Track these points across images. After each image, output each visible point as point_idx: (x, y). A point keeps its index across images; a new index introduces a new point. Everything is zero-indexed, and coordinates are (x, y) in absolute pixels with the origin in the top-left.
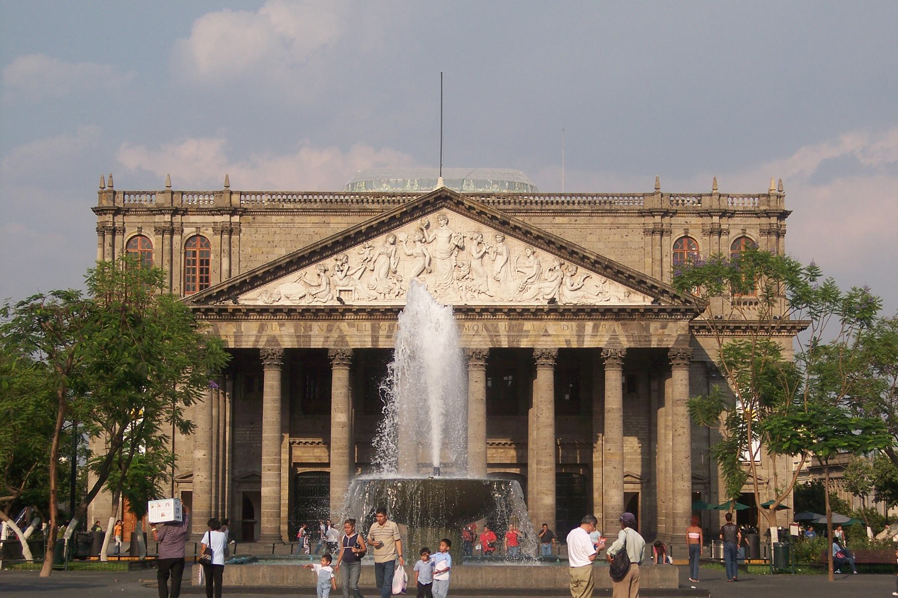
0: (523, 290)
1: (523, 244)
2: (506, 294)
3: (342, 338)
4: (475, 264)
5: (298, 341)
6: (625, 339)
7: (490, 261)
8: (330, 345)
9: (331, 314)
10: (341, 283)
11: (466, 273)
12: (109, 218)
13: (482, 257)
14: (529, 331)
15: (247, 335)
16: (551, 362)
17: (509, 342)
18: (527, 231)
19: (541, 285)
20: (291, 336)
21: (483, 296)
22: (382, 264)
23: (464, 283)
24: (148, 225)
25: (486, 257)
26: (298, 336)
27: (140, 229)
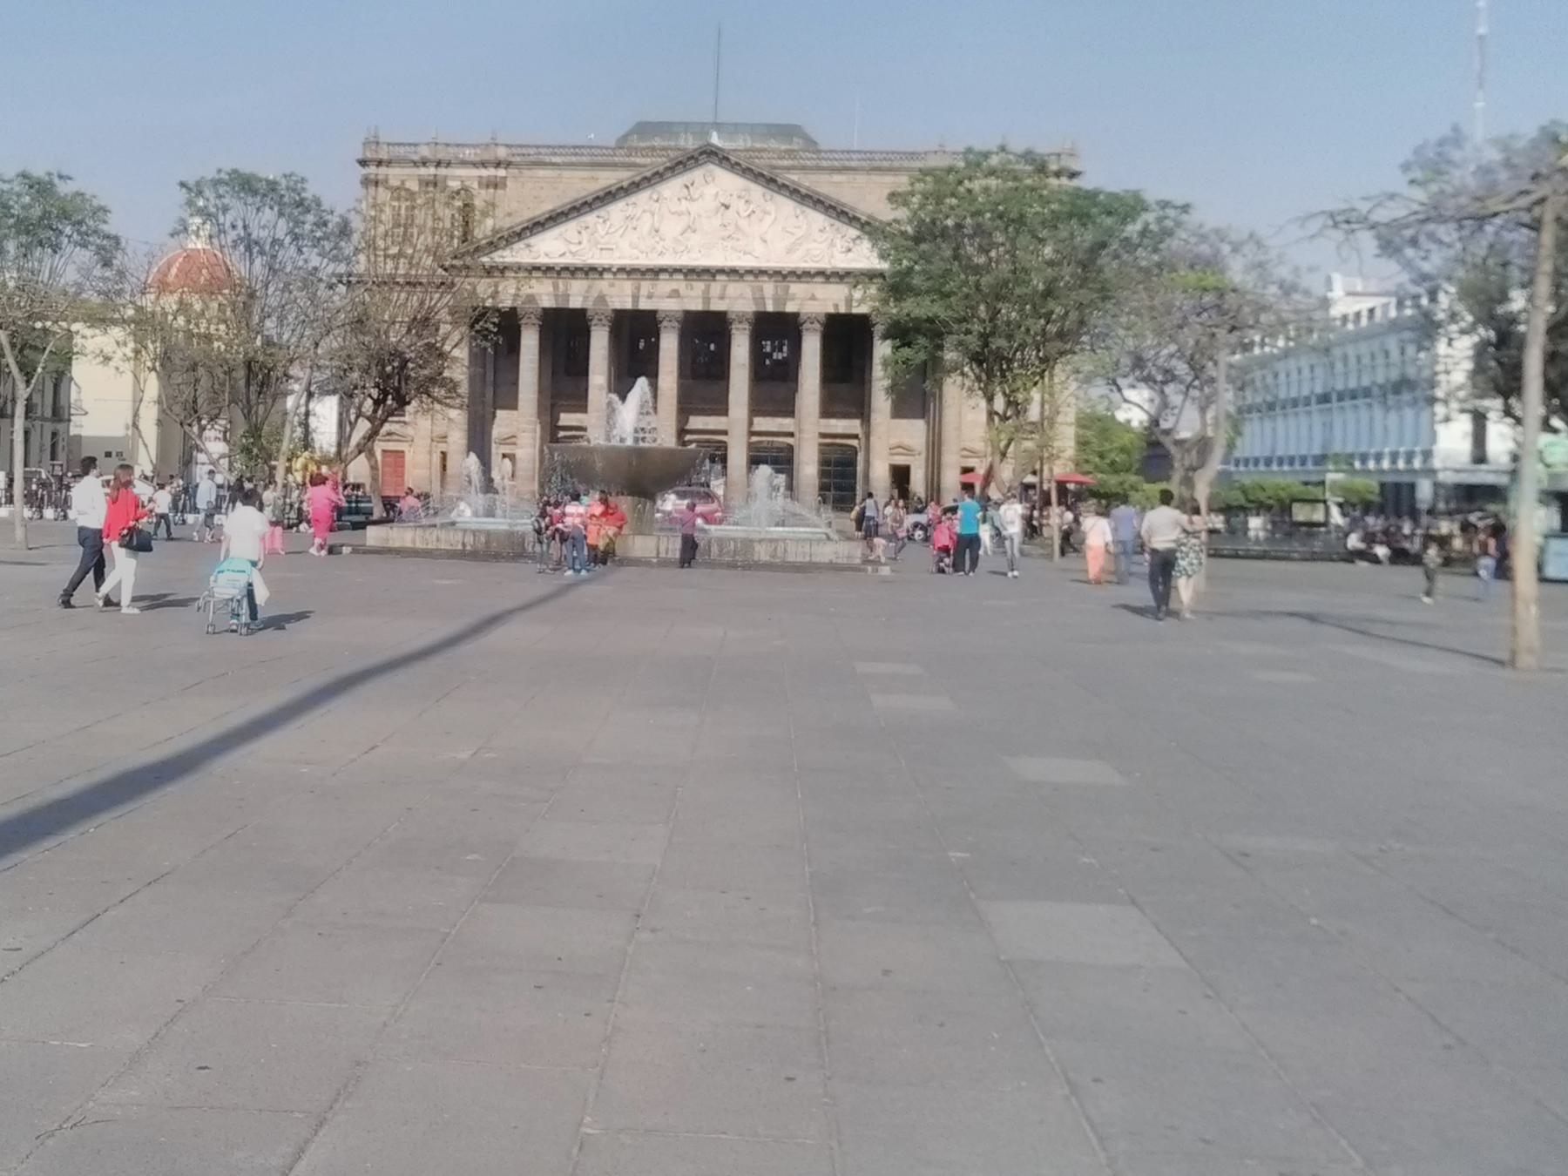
0: (789, 251)
3: (601, 298)
4: (743, 223)
8: (589, 305)
12: (372, 170)
16: (817, 326)
22: (645, 224)
23: (729, 244)
24: (410, 178)
26: (556, 296)
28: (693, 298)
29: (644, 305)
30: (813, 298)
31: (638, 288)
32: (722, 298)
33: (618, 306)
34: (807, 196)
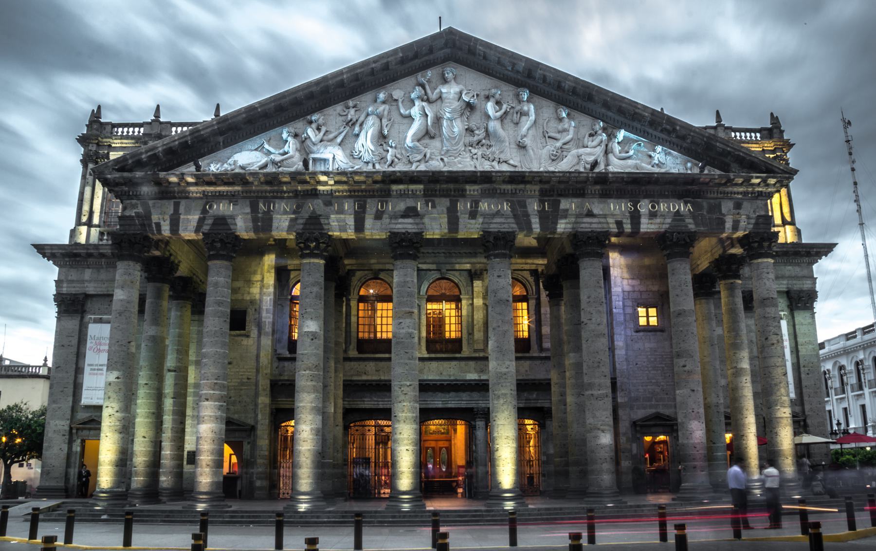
0: (555, 158)
1: (552, 104)
2: (539, 160)
4: (494, 125)
6: (691, 221)
7: (512, 125)
11: (481, 137)
13: (502, 119)
14: (567, 210)
17: (541, 224)
21: (504, 164)
25: (507, 121)
30: (590, 214)
32: (473, 215)
34: (574, 91)
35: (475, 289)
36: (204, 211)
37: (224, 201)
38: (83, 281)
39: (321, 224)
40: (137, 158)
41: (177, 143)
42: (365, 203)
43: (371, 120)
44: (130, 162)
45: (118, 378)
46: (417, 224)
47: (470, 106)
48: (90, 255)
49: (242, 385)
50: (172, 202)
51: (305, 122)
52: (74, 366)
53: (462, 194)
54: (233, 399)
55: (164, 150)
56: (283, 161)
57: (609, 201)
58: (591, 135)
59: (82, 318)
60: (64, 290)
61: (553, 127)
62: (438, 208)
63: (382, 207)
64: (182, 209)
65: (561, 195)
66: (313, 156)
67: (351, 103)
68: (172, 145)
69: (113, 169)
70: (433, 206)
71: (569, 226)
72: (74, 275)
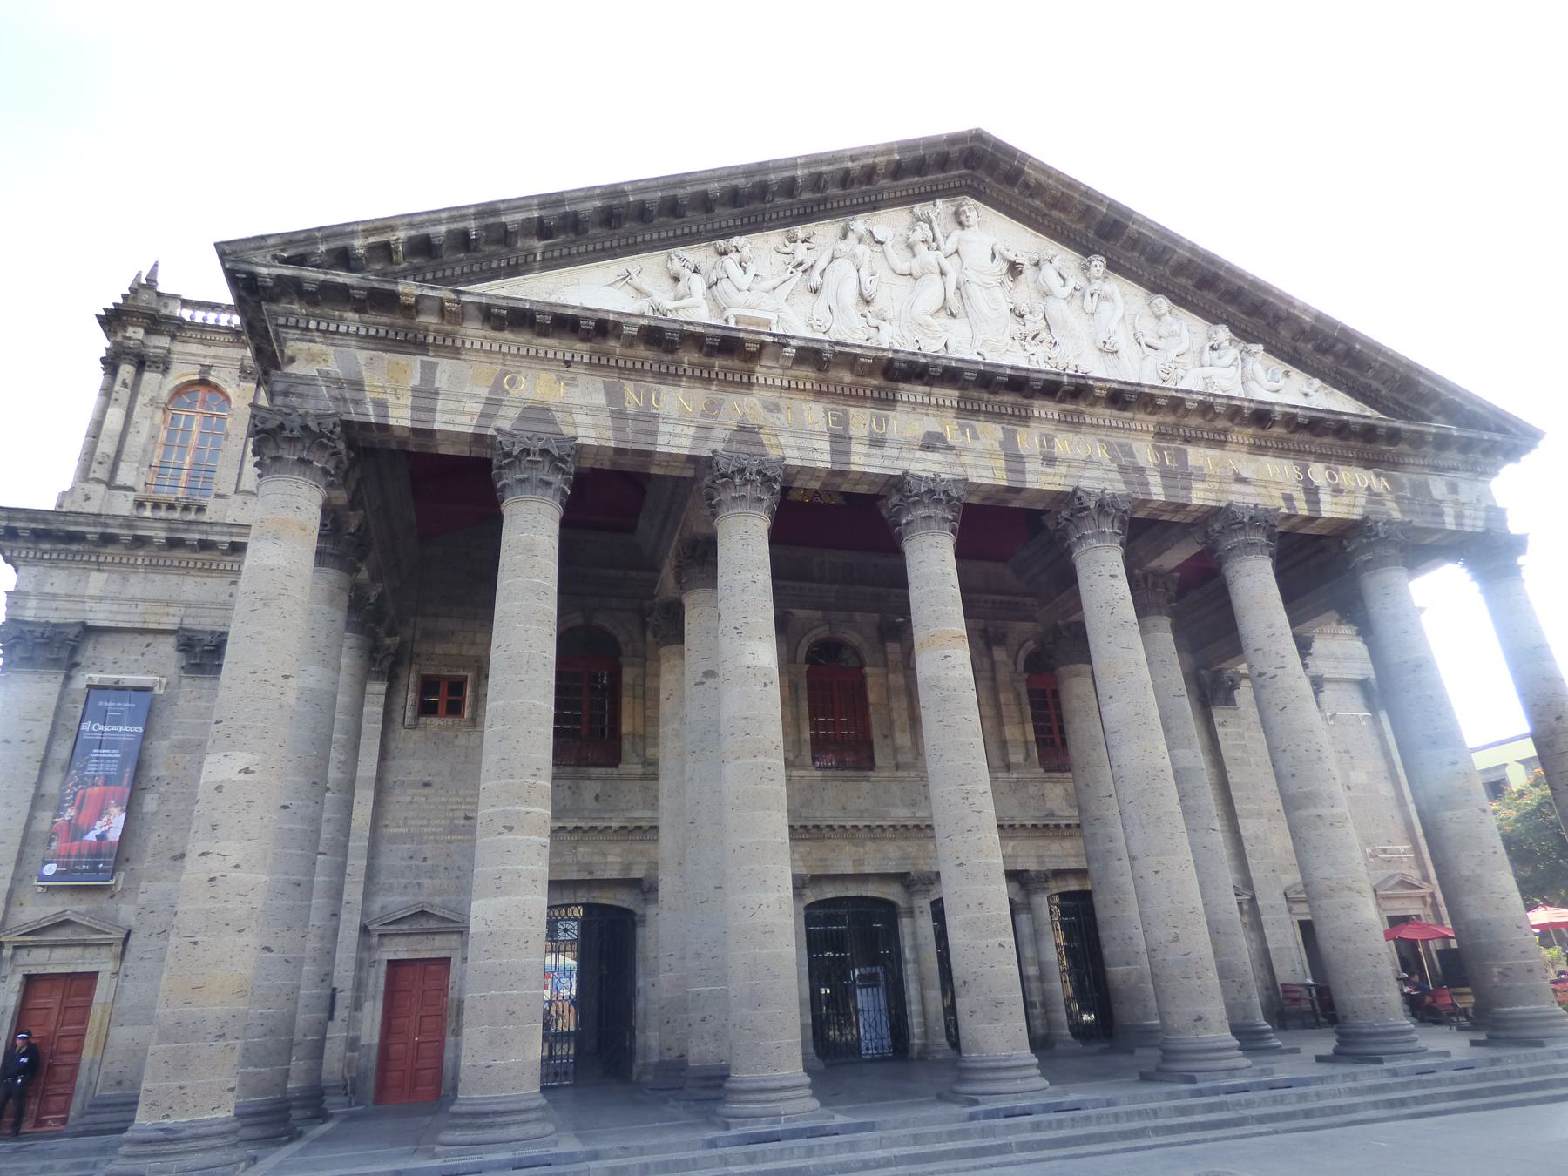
4: (1057, 308)
5: (618, 429)
6: (1394, 505)
8: (716, 444)
9: (728, 353)
10: (741, 298)
12: (136, 333)
14: (1201, 469)
15: (459, 394)
17: (1165, 487)
18: (1165, 249)
19: (1207, 371)
20: (593, 410)
26: (619, 415)
27: (207, 368)
28: (978, 456)
29: (863, 461)
30: (1241, 480)
31: (844, 422)
32: (1050, 460)
33: (794, 459)
34: (1183, 268)
35: (891, 657)
36: (497, 387)
37: (543, 375)
38: (82, 599)
39: (762, 445)
40: (339, 243)
41: (443, 229)
42: (846, 413)
43: (844, 267)
44: (322, 248)
45: (247, 771)
46: (950, 465)
47: (1014, 269)
48: (107, 540)
49: (452, 833)
50: (416, 361)
51: (711, 251)
52: (32, 790)
53: (1025, 419)
54: (430, 862)
55: (410, 239)
56: (677, 310)
57: (1263, 459)
58: (1213, 348)
59: (68, 678)
60: (30, 613)
61: (1148, 327)
62: (983, 440)
63: (879, 426)
64: (441, 381)
65: (1187, 440)
66: (730, 313)
67: (800, 231)
68: (431, 230)
69: (275, 257)
70: (975, 436)
71: (1213, 496)
72: (59, 580)
